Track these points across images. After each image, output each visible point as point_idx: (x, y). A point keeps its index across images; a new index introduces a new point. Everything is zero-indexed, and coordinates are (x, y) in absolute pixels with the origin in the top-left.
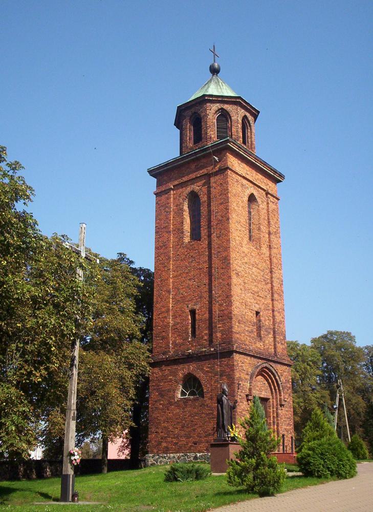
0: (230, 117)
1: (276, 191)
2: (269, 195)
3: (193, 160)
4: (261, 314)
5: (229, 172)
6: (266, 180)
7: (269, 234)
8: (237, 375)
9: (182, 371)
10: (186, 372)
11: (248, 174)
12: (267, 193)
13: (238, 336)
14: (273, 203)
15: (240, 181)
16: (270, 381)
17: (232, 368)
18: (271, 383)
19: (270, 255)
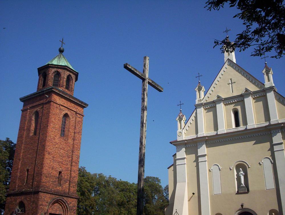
0: (61, 76)
1: (83, 112)
2: (77, 114)
3: (38, 95)
4: (63, 172)
5: (52, 103)
6: (76, 107)
7: (75, 133)
8: (40, 203)
9: (19, 199)
10: (20, 200)
11: (65, 104)
12: (76, 113)
13: (44, 184)
14: (79, 117)
15: (59, 106)
16: (63, 206)
17: (38, 199)
18: (64, 207)
19: (73, 143)
